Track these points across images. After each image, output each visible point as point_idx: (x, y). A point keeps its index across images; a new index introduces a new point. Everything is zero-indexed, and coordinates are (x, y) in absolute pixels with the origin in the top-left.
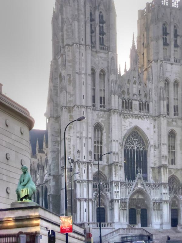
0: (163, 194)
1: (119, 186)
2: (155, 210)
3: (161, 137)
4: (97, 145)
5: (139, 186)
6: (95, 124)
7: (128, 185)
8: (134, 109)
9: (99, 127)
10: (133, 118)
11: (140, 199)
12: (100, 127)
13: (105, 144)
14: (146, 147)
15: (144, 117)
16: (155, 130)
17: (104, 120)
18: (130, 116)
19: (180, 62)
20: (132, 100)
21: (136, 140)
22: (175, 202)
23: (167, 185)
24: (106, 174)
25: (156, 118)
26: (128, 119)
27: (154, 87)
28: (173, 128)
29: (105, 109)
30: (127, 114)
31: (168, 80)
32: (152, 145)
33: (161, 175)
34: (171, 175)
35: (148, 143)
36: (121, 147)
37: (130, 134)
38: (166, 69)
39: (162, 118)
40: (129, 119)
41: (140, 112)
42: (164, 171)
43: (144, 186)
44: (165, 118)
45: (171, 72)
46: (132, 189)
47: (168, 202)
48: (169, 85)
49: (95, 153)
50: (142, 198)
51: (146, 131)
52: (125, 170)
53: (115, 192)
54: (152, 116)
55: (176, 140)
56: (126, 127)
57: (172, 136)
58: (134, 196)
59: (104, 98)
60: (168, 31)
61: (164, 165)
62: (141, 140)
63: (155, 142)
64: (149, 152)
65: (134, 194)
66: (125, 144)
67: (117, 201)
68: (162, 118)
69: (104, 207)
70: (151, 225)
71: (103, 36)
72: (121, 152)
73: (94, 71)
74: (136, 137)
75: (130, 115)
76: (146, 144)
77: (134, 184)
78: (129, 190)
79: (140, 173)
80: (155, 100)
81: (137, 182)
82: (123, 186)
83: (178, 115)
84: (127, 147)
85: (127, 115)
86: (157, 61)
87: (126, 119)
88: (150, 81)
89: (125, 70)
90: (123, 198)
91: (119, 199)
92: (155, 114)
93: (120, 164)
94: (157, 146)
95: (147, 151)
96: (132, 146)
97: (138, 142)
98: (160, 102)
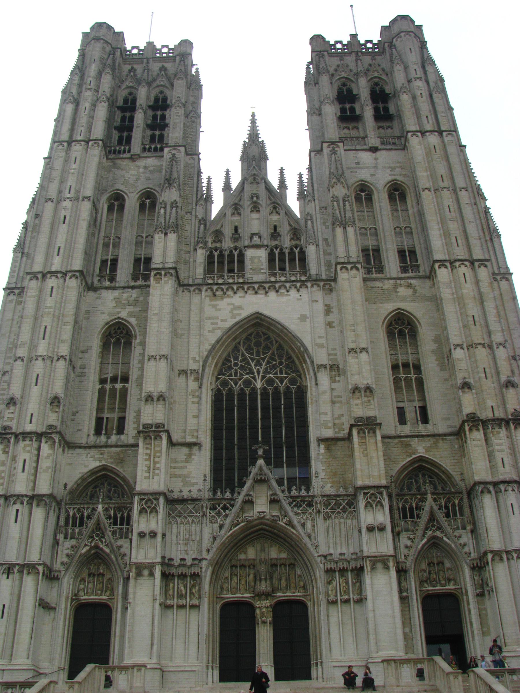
6: (107, 324)
8: (251, 269)
10: (246, 293)
14: (303, 375)
15: (288, 285)
17: (138, 309)
18: (233, 289)
20: (245, 247)
21: (263, 359)
25: (332, 283)
26: (226, 300)
27: (321, 208)
35: (305, 361)
37: (239, 343)
40: (229, 296)
41: (274, 275)
50: (284, 555)
53: (142, 535)
54: (316, 281)
63: (336, 355)
67: (146, 572)
71: (164, 130)
72: (196, 400)
75: (235, 287)
78: (216, 526)
80: (326, 240)
84: (225, 383)
85: (222, 290)
86: (322, 150)
87: (222, 299)
89: (227, 187)
92: (327, 275)
95: (306, 386)
96: (248, 376)
97: (268, 362)
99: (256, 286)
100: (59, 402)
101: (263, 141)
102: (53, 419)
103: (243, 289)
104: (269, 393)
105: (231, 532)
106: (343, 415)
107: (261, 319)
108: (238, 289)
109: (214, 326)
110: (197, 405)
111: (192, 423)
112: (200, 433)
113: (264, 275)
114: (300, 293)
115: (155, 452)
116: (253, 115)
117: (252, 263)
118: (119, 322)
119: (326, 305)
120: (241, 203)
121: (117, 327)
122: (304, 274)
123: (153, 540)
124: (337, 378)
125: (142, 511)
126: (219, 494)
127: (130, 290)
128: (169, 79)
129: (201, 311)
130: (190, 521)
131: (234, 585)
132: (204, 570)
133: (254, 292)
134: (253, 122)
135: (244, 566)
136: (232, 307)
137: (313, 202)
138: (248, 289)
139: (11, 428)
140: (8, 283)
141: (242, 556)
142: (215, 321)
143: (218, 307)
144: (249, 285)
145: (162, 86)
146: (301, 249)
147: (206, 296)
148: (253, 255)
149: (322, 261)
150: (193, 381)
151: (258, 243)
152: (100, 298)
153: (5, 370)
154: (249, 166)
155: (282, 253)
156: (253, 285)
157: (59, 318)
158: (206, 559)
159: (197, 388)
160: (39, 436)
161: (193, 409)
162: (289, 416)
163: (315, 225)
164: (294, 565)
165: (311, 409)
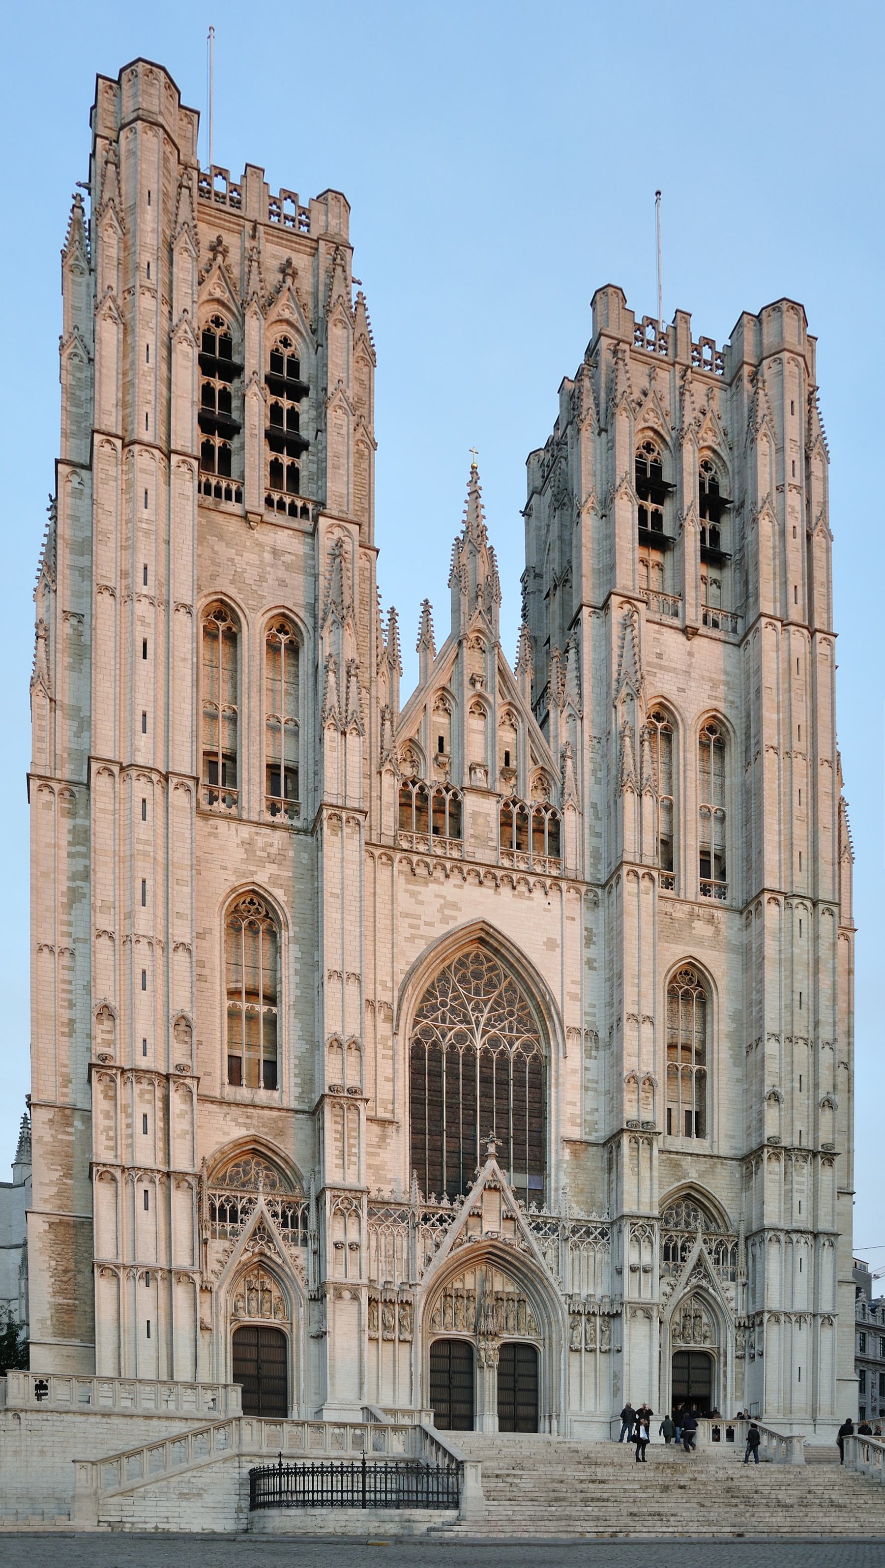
0: (626, 1271)
1: (364, 1214)
2: (577, 1351)
3: (621, 985)
4: (244, 1005)
5: (491, 1224)
7: (426, 1219)
8: (473, 836)
10: (465, 879)
13: (292, 998)
15: (532, 879)
16: (592, 952)
18: (444, 868)
19: (734, 630)
20: (462, 789)
21: (486, 1003)
24: (293, 1157)
25: (599, 891)
26: (432, 886)
29: (298, 823)
30: (428, 860)
33: (619, 1178)
36: (388, 1026)
37: (449, 967)
38: (660, 656)
40: (436, 881)
41: (510, 855)
43: (518, 1229)
44: (645, 883)
46: (448, 1241)
49: (237, 1053)
52: (416, 1148)
56: (423, 927)
58: (463, 1281)
59: (292, 772)
60: (667, 476)
62: (511, 1003)
65: (458, 1267)
66: (420, 1014)
68: (629, 886)
69: (276, 1321)
70: (554, 1422)
72: (391, 1053)
79: (503, 1164)
81: (479, 1204)
82: (395, 1221)
84: (426, 1032)
85: (427, 865)
87: (426, 884)
89: (425, 643)
93: (382, 1114)
97: (492, 1009)
99: (482, 871)
101: (491, 548)
103: (461, 871)
104: (492, 1058)
105: (453, 1253)
107: (487, 933)
109: (413, 931)
111: (385, 1091)
113: (495, 853)
114: (549, 898)
116: (474, 470)
117: (475, 823)
118: (253, 891)
119: (586, 929)
120: (453, 689)
121: (248, 900)
122: (557, 864)
124: (594, 1053)
126: (433, 1199)
132: (418, 1298)
133: (477, 881)
134: (475, 494)
136: (442, 901)
137: (579, 722)
142: (415, 922)
143: (420, 898)
146: (554, 814)
147: (400, 872)
148: (475, 809)
149: (586, 845)
150: (384, 1021)
156: (477, 868)
161: (385, 1068)
162: (519, 1099)
163: (579, 771)
165: (553, 1094)
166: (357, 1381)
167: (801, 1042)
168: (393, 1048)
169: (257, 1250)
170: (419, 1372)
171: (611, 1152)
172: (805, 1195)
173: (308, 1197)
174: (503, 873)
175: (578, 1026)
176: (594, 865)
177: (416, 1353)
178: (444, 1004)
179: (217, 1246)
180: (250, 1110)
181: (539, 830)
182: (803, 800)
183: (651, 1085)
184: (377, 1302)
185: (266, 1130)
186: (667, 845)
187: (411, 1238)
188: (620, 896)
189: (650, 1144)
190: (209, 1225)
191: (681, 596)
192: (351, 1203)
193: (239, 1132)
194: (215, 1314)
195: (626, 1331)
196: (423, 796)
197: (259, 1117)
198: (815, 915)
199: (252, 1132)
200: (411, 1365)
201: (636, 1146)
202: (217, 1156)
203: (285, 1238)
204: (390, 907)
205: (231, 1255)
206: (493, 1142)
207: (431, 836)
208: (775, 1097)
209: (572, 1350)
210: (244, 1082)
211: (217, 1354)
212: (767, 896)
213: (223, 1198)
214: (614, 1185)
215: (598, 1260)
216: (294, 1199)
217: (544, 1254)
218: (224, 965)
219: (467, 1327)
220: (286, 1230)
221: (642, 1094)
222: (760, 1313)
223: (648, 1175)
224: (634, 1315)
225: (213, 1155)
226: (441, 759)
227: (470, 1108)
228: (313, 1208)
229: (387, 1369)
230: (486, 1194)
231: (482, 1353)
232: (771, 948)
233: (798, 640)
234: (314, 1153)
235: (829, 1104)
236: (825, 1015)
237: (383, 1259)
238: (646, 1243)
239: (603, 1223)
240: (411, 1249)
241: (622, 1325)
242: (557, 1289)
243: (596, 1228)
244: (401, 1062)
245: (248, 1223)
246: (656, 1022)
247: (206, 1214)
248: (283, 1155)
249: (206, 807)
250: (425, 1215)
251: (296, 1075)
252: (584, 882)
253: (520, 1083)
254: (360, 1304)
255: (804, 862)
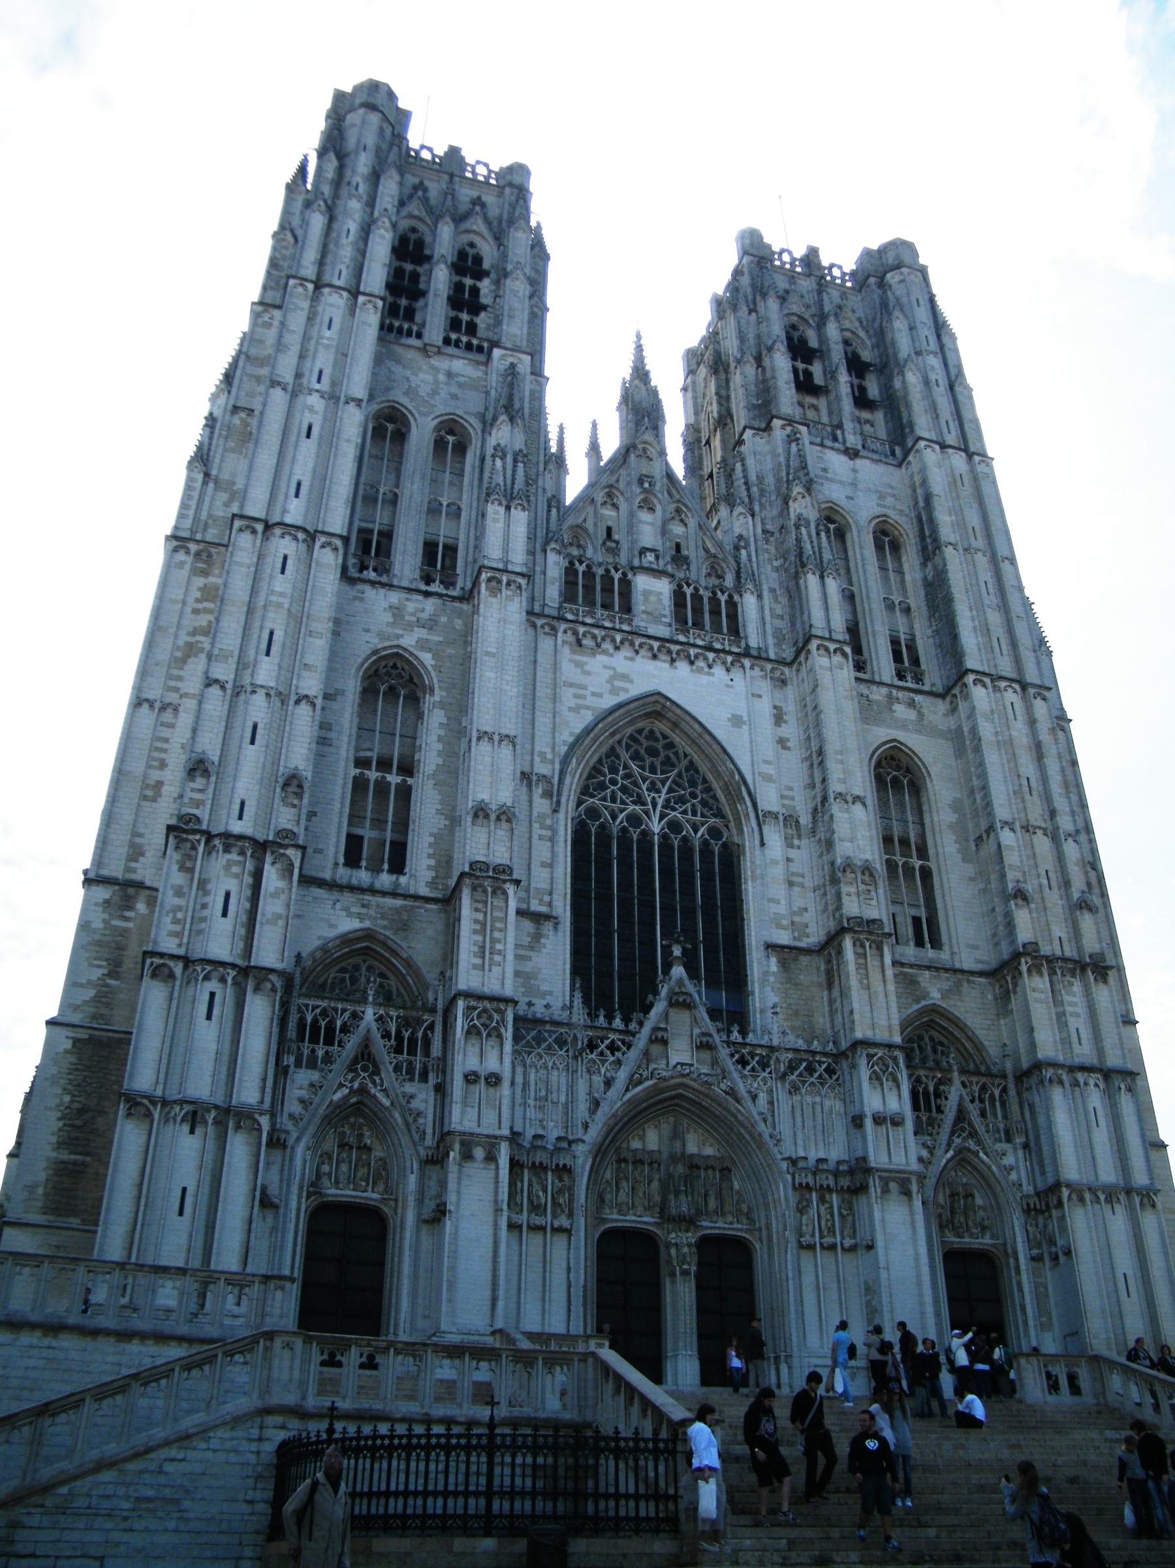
0: (868, 1123)
4: (373, 775)
6: (375, 652)
7: (592, 1046)
8: (644, 612)
9: (400, 676)
10: (637, 652)
11: (694, 1164)
12: (411, 680)
13: (433, 767)
14: (732, 825)
15: (711, 656)
18: (613, 641)
19: (893, 453)
20: (632, 568)
21: (663, 782)
22: (969, 1195)
23: (895, 1059)
25: (786, 670)
26: (601, 659)
28: (901, 736)
29: (455, 593)
31: (837, 518)
32: (774, 816)
33: (845, 994)
34: (916, 1007)
37: (619, 742)
38: (825, 470)
39: (820, 661)
40: (605, 652)
41: (685, 632)
42: (863, 967)
43: (715, 1062)
45: (854, 485)
46: (622, 1075)
47: (914, 1188)
48: (848, 536)
49: (358, 831)
51: (721, 731)
53: (471, 1078)
54: (759, 657)
55: (925, 808)
57: (895, 780)
58: (642, 1138)
61: (859, 920)
62: (693, 784)
63: (793, 799)
64: (752, 848)
66: (585, 791)
67: (479, 1153)
68: (820, 661)
69: (375, 1196)
70: (784, 1369)
71: (477, 314)
72: (549, 833)
73: (407, 424)
74: (658, 763)
75: (618, 637)
76: (727, 810)
77: (646, 1031)
78: (598, 1080)
80: (772, 590)
82: (549, 1047)
83: (918, 679)
84: (593, 813)
85: (594, 637)
87: (594, 655)
88: (739, 509)
89: (594, 449)
90: (541, 1137)
91: (502, 1138)
93: (535, 906)
94: (805, 820)
97: (670, 791)
98: (801, 582)
99: (656, 645)
100: (300, 786)
102: (285, 818)
103: (632, 644)
105: (629, 1095)
106: (806, 910)
108: (622, 642)
109: (579, 701)
110: (549, 844)
111: (539, 878)
112: (555, 897)
114: (732, 675)
115: (493, 920)
117: (646, 599)
118: (397, 655)
119: (775, 707)
123: (492, 1090)
125: (471, 1032)
126: (602, 1019)
127: (420, 598)
128: (487, 222)
129: (556, 667)
130: (550, 1064)
131: (622, 1196)
132: (580, 1161)
135: (642, 1162)
138: (641, 646)
139: (198, 820)
140: (176, 528)
141: (636, 1144)
142: (581, 692)
143: (587, 668)
144: (643, 640)
145: (474, 232)
147: (564, 642)
151: (655, 566)
152: (362, 600)
153: (167, 700)
154: (638, 423)
155: (696, 597)
156: (652, 642)
157: (299, 620)
158: (583, 1141)
159: (549, 811)
160: (260, 848)
164: (730, 1170)
166: (487, 1294)
167: (1039, 832)
168: (551, 828)
169: (356, 1085)
170: (582, 1282)
171: (829, 962)
172: (1081, 1020)
173: (433, 1010)
174: (678, 647)
175: (775, 809)
176: (778, 645)
177: (577, 1249)
178: (614, 782)
179: (303, 1078)
180: (367, 897)
181: (715, 612)
182: (991, 590)
183: (871, 875)
184: (522, 1166)
185: (385, 923)
186: (853, 630)
187: (571, 1072)
188: (811, 670)
189: (880, 949)
190: (294, 1047)
191: (840, 426)
192: (490, 1018)
193: (349, 925)
194: (285, 1181)
195: (877, 1215)
196: (589, 574)
197: (378, 906)
198: (1024, 698)
199: (367, 924)
200: (569, 1270)
201: (860, 950)
202: (318, 954)
203: (397, 1069)
204: (550, 676)
205: (320, 1092)
206: (678, 942)
207: (599, 612)
208: (1021, 895)
209: (801, 1246)
210: (364, 863)
211: (282, 1247)
212: (970, 678)
213: (318, 1011)
214: (838, 1004)
215: (826, 1108)
216: (414, 1014)
217: (754, 1098)
218: (355, 730)
219: (648, 1208)
220: (401, 1058)
221: (862, 887)
222: (1056, 1186)
223: (880, 989)
224: (885, 1190)
225: (312, 954)
226: (610, 544)
227: (647, 905)
228: (438, 1028)
229: (533, 1276)
230: (674, 1014)
231: (673, 1252)
232: (986, 730)
233: (958, 460)
234: (445, 954)
235: (1084, 905)
236: (1060, 803)
237: (531, 1102)
238: (890, 1083)
239: (825, 1054)
240: (571, 1088)
241: (869, 1205)
242: (775, 1150)
243: (820, 1063)
244: (562, 844)
245: (349, 1046)
246: (869, 802)
247: (292, 1033)
248: (404, 955)
249: (353, 573)
250: (590, 1040)
251: (429, 856)
252: (768, 660)
253: (708, 878)
254: (497, 1168)
255: (1004, 648)
